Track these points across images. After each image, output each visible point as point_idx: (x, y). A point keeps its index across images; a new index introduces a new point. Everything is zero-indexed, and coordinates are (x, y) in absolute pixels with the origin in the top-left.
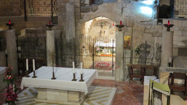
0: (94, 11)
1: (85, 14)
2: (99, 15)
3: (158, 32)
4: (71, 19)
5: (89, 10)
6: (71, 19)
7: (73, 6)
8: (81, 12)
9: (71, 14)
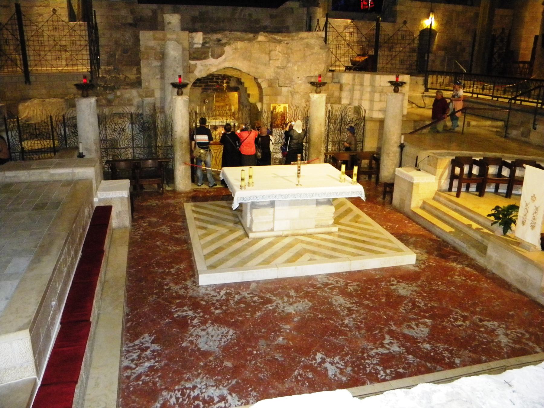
0: (217, 58)
1: (198, 62)
3: (333, 95)
7: (180, 47)
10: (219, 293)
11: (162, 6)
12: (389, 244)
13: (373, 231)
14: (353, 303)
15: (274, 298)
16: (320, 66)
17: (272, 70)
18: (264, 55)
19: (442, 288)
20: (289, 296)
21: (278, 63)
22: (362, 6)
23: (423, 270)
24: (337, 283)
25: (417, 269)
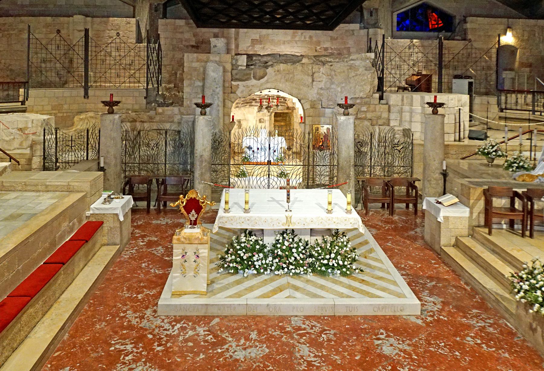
0: (259, 80)
2: (269, 85)
4: (218, 93)
5: (248, 76)
6: (218, 93)
8: (232, 80)
9: (217, 84)
10: (173, 326)
11: (222, 30)
12: (392, 287)
13: (380, 269)
14: (319, 356)
15: (230, 339)
16: (366, 87)
17: (316, 91)
18: (306, 77)
19: (442, 352)
20: (247, 339)
21: (322, 85)
22: (430, 26)
23: (428, 324)
24: (312, 329)
25: (420, 322)
